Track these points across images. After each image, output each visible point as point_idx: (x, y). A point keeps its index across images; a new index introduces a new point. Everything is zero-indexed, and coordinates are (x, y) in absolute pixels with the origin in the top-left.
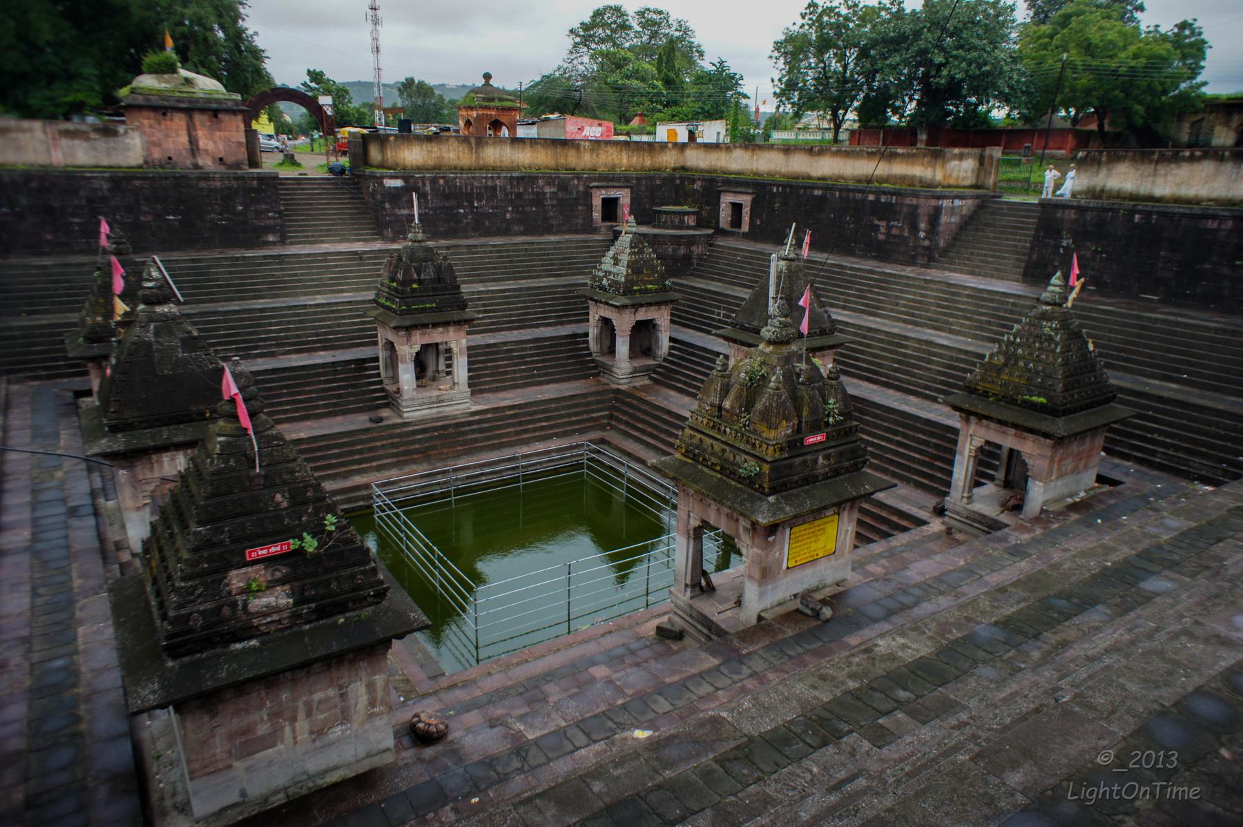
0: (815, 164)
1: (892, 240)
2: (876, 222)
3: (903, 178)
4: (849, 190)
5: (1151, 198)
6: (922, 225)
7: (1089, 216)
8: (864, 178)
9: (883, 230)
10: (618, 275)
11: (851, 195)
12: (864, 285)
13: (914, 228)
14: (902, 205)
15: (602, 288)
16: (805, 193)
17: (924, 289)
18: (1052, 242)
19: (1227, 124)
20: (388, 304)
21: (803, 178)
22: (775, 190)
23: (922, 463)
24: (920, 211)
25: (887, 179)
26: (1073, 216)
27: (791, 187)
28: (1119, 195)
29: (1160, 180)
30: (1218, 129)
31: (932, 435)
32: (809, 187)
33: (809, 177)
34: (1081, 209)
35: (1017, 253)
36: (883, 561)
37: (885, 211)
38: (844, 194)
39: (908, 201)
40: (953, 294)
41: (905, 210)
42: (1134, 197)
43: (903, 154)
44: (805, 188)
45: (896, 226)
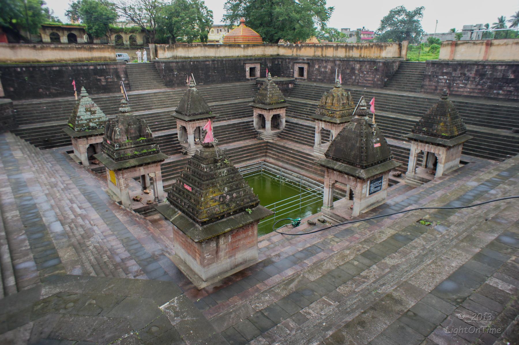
0: (41, 54)
1: (110, 84)
2: (99, 78)
3: (100, 58)
4: (77, 66)
5: (189, 58)
6: (122, 76)
7: (179, 64)
8: (78, 59)
9: (103, 80)
10: (101, 118)
11: (79, 68)
12: (133, 101)
13: (119, 77)
14: (109, 69)
15: (93, 128)
16: (46, 70)
17: (157, 96)
18: (172, 74)
19: (45, 33)
20: (145, 151)
21: (33, 62)
22: (19, 70)
23: (239, 134)
24: (119, 70)
25: (92, 59)
26: (175, 65)
27: (34, 67)
28: (181, 58)
29: (190, 52)
30: (43, 35)
31: (232, 127)
32: (49, 66)
33: (38, 62)
34: (177, 62)
35: (154, 80)
37: (103, 72)
38: (74, 68)
39: (112, 67)
40: (168, 95)
41: (112, 71)
42: (185, 58)
43: (97, 48)
44: (45, 67)
45: (110, 78)
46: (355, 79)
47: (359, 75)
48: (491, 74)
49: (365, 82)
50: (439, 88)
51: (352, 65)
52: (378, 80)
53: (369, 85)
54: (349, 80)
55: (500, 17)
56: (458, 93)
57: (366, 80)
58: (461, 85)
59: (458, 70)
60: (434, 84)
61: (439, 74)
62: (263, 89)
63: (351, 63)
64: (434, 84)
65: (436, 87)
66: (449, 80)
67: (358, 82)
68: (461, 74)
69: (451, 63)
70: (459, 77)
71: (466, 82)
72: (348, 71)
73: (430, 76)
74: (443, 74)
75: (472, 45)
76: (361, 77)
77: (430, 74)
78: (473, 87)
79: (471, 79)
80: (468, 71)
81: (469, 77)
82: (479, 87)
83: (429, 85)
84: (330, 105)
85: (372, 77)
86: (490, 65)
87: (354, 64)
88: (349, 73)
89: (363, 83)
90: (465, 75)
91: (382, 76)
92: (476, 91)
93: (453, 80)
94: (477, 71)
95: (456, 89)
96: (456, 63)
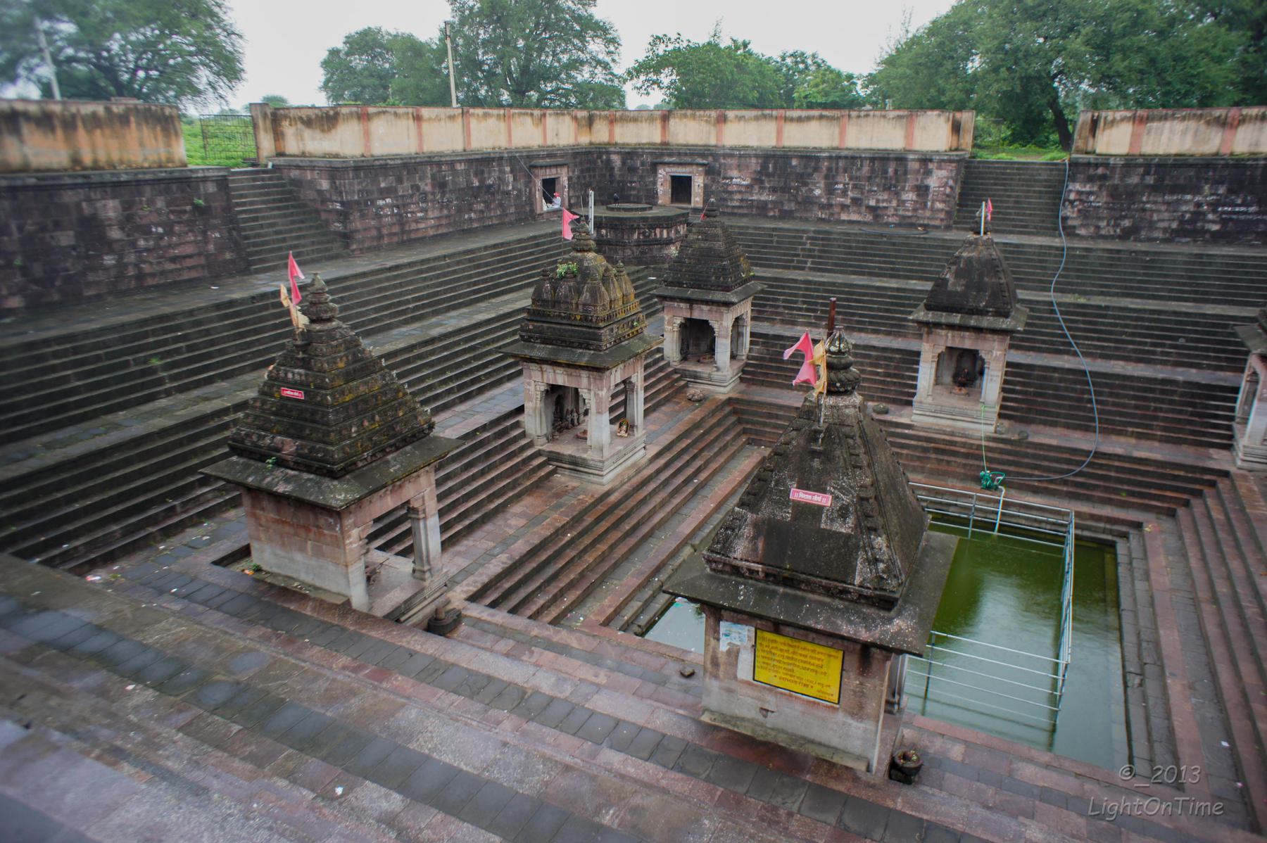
36: (511, 532)
46: (121, 266)
47: (133, 244)
48: (453, 181)
49: (169, 266)
50: (385, 231)
51: (78, 205)
52: (221, 249)
53: (194, 274)
54: (91, 277)
55: (324, 55)
56: (420, 235)
57: (174, 259)
58: (419, 215)
59: (405, 178)
60: (373, 223)
61: (376, 195)
62: (349, 376)
63: (69, 197)
64: (373, 223)
65: (379, 230)
66: (398, 207)
67: (141, 276)
68: (412, 187)
69: (392, 162)
70: (412, 196)
71: (424, 205)
72: (66, 238)
73: (357, 203)
74: (384, 193)
75: (393, 117)
76: (147, 250)
77: (356, 198)
78: (437, 213)
79: (430, 197)
80: (421, 179)
81: (425, 194)
82: (445, 212)
83: (365, 230)
84: (621, 303)
85: (196, 242)
86: (447, 163)
87: (88, 200)
88: (74, 248)
89: (163, 273)
90: (418, 188)
91: (229, 231)
92: (444, 222)
93: (405, 206)
94: (433, 177)
95: (414, 226)
96: (399, 162)
